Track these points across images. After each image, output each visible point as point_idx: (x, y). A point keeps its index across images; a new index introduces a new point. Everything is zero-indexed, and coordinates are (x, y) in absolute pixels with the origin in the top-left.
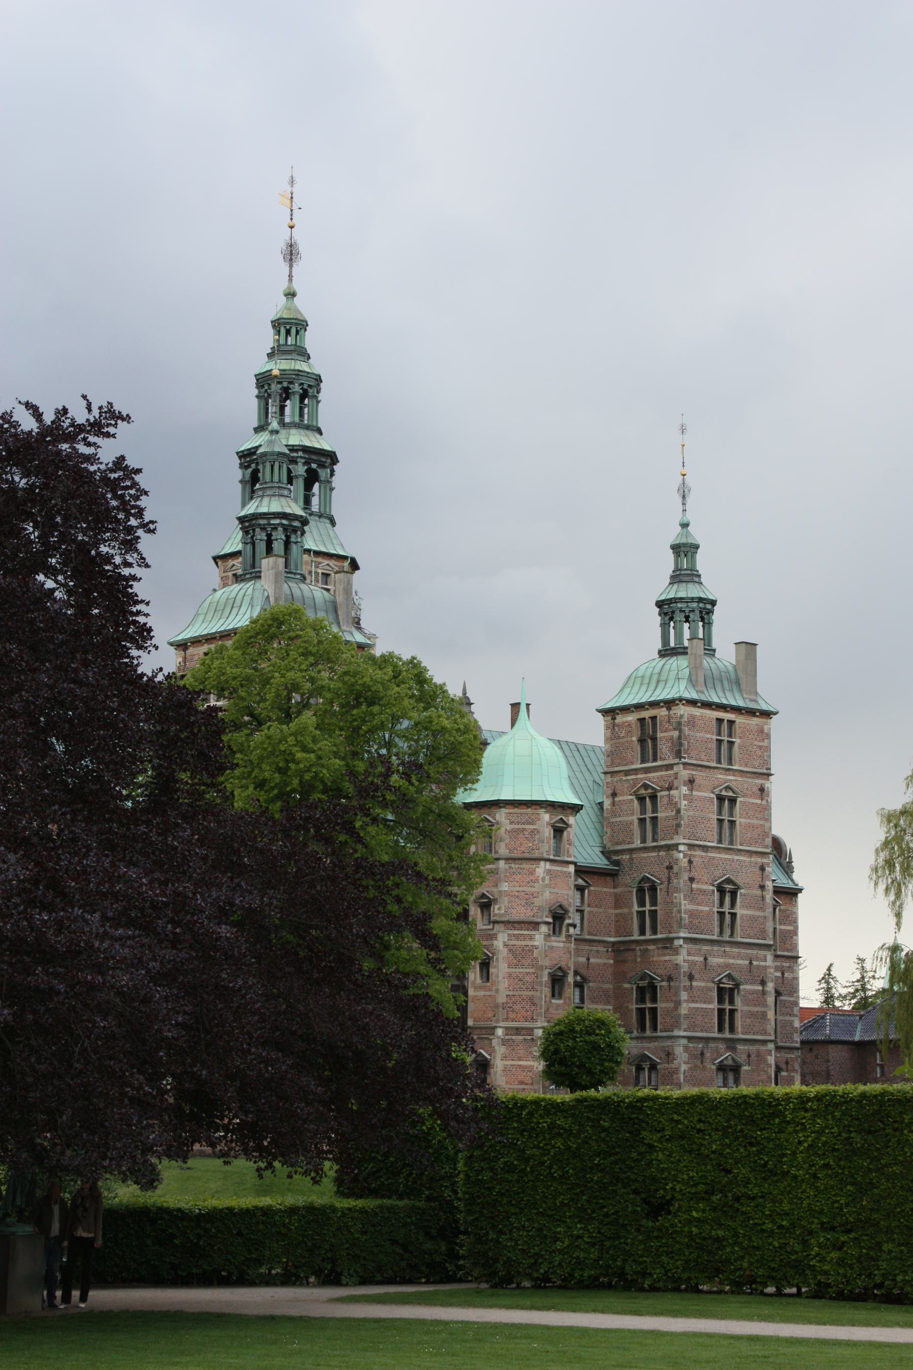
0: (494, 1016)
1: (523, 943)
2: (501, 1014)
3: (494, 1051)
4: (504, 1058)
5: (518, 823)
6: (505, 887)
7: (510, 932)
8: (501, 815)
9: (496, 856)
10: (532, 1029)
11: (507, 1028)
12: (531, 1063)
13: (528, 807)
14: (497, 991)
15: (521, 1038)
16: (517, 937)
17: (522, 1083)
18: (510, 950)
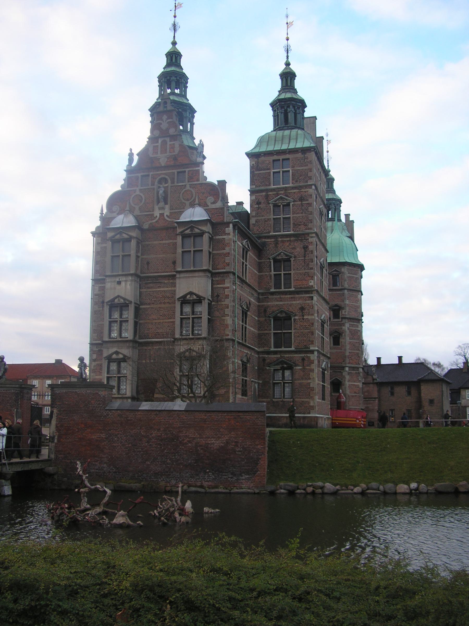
0: (344, 361)
1: (354, 328)
2: (347, 360)
3: (344, 377)
4: (349, 381)
5: (351, 274)
6: (347, 302)
7: (350, 323)
8: (344, 270)
9: (343, 288)
10: (358, 368)
11: (349, 367)
12: (359, 384)
13: (355, 267)
14: (345, 350)
15: (355, 372)
16: (352, 326)
17: (355, 393)
18: (350, 331)
